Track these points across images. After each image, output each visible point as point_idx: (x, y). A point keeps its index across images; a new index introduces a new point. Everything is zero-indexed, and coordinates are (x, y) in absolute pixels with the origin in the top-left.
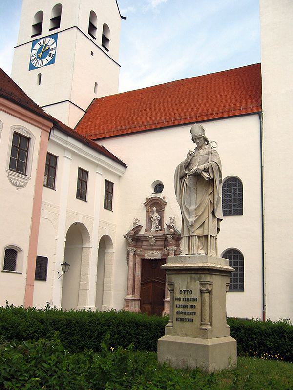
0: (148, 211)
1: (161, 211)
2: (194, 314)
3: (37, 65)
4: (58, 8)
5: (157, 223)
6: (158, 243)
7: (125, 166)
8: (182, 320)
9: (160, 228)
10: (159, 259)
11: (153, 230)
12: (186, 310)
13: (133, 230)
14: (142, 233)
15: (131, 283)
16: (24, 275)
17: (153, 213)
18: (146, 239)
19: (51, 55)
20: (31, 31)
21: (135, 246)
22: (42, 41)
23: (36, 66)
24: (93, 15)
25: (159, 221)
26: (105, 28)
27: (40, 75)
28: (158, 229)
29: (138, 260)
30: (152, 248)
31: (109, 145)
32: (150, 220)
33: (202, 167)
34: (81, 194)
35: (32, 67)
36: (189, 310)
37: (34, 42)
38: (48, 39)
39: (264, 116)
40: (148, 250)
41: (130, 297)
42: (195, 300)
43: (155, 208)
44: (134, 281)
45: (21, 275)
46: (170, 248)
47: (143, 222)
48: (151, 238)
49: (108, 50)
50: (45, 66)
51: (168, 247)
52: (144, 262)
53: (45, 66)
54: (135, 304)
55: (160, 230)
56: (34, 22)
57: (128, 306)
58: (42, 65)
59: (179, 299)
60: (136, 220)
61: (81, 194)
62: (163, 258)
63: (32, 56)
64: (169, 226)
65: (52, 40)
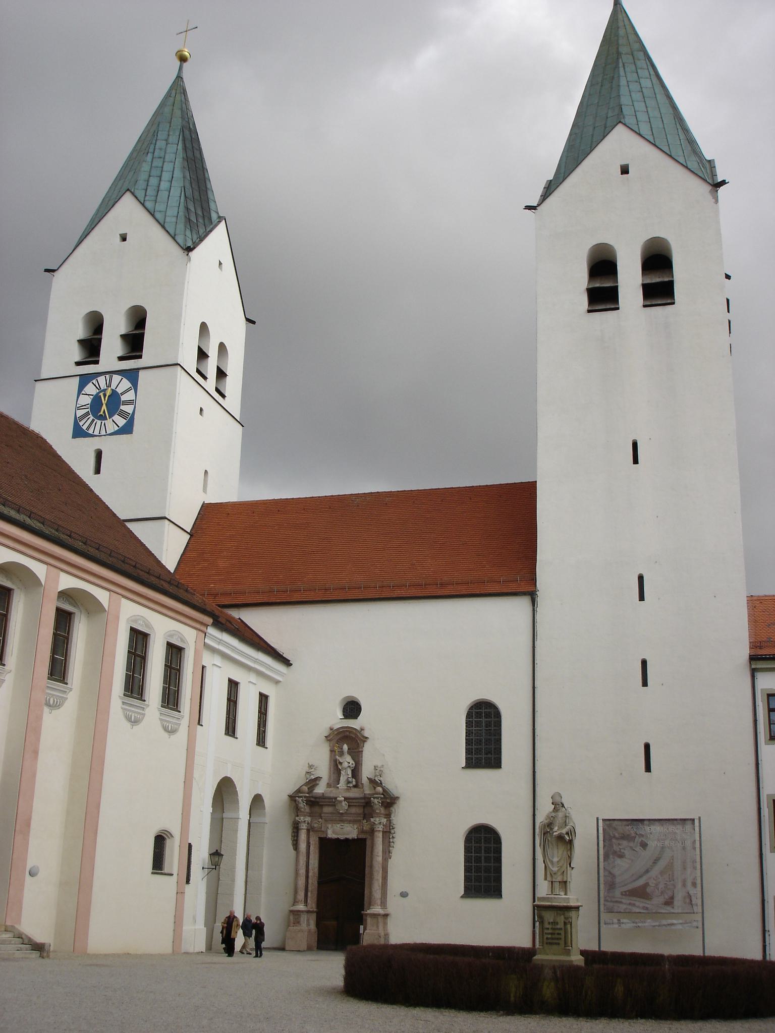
0: (332, 751)
2: (561, 939)
3: (88, 428)
4: (138, 318)
5: (349, 772)
6: (353, 810)
7: (287, 663)
8: (551, 944)
9: (354, 783)
10: (353, 840)
11: (342, 784)
12: (554, 936)
13: (306, 784)
14: (320, 789)
15: (302, 882)
17: (342, 754)
18: (332, 802)
19: (123, 414)
20: (77, 354)
21: (311, 815)
22: (102, 380)
23: (91, 431)
24: (204, 327)
25: (352, 770)
26: (222, 347)
27: (99, 455)
28: (351, 785)
29: (314, 841)
30: (341, 818)
31: (256, 619)
32: (336, 769)
33: (564, 831)
34: (231, 729)
35: (79, 432)
36: (556, 936)
37: (85, 380)
38: (116, 378)
39: (540, 600)
40: (333, 821)
41: (301, 907)
42: (561, 929)
43: (345, 747)
44: (307, 877)
45: (171, 877)
46: (376, 820)
47: (323, 770)
48: (341, 802)
49: (223, 396)
50: (110, 434)
51: (372, 820)
52: (326, 845)
53: (110, 434)
54: (308, 920)
55: (355, 786)
56: (81, 332)
57: (299, 922)
58: (103, 432)
59: (548, 929)
60: (311, 767)
61: (231, 729)
62: (360, 837)
64: (372, 781)
65: (126, 384)
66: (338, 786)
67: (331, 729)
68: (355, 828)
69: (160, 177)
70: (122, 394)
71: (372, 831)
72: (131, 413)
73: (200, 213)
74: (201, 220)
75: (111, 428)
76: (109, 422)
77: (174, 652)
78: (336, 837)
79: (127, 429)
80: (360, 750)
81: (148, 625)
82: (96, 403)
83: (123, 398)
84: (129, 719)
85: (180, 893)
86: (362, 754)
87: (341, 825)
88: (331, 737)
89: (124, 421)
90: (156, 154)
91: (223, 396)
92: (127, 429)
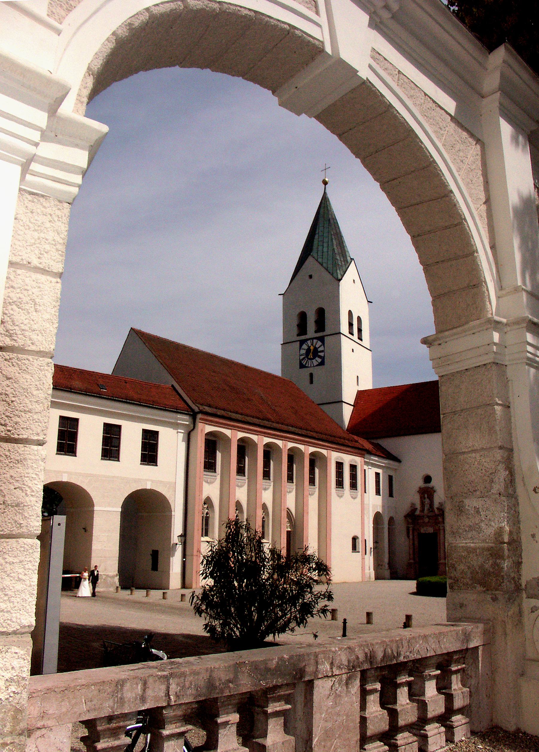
1: (431, 498)
4: (321, 312)
7: (399, 461)
11: (426, 511)
14: (418, 513)
16: (360, 553)
19: (320, 357)
22: (309, 342)
23: (307, 365)
26: (359, 319)
27: (311, 375)
29: (416, 534)
32: (423, 504)
34: (378, 492)
35: (302, 366)
37: (302, 342)
38: (315, 341)
41: (412, 561)
43: (426, 495)
47: (418, 506)
49: (361, 340)
63: (300, 355)
65: (319, 343)
67: (420, 488)
69: (323, 246)
70: (319, 347)
71: (439, 530)
72: (323, 356)
73: (342, 260)
74: (343, 263)
75: (315, 363)
76: (314, 361)
77: (353, 468)
79: (322, 363)
81: (342, 459)
82: (308, 350)
83: (319, 350)
84: (338, 496)
85: (363, 559)
89: (321, 360)
90: (320, 234)
91: (361, 340)
92: (322, 363)
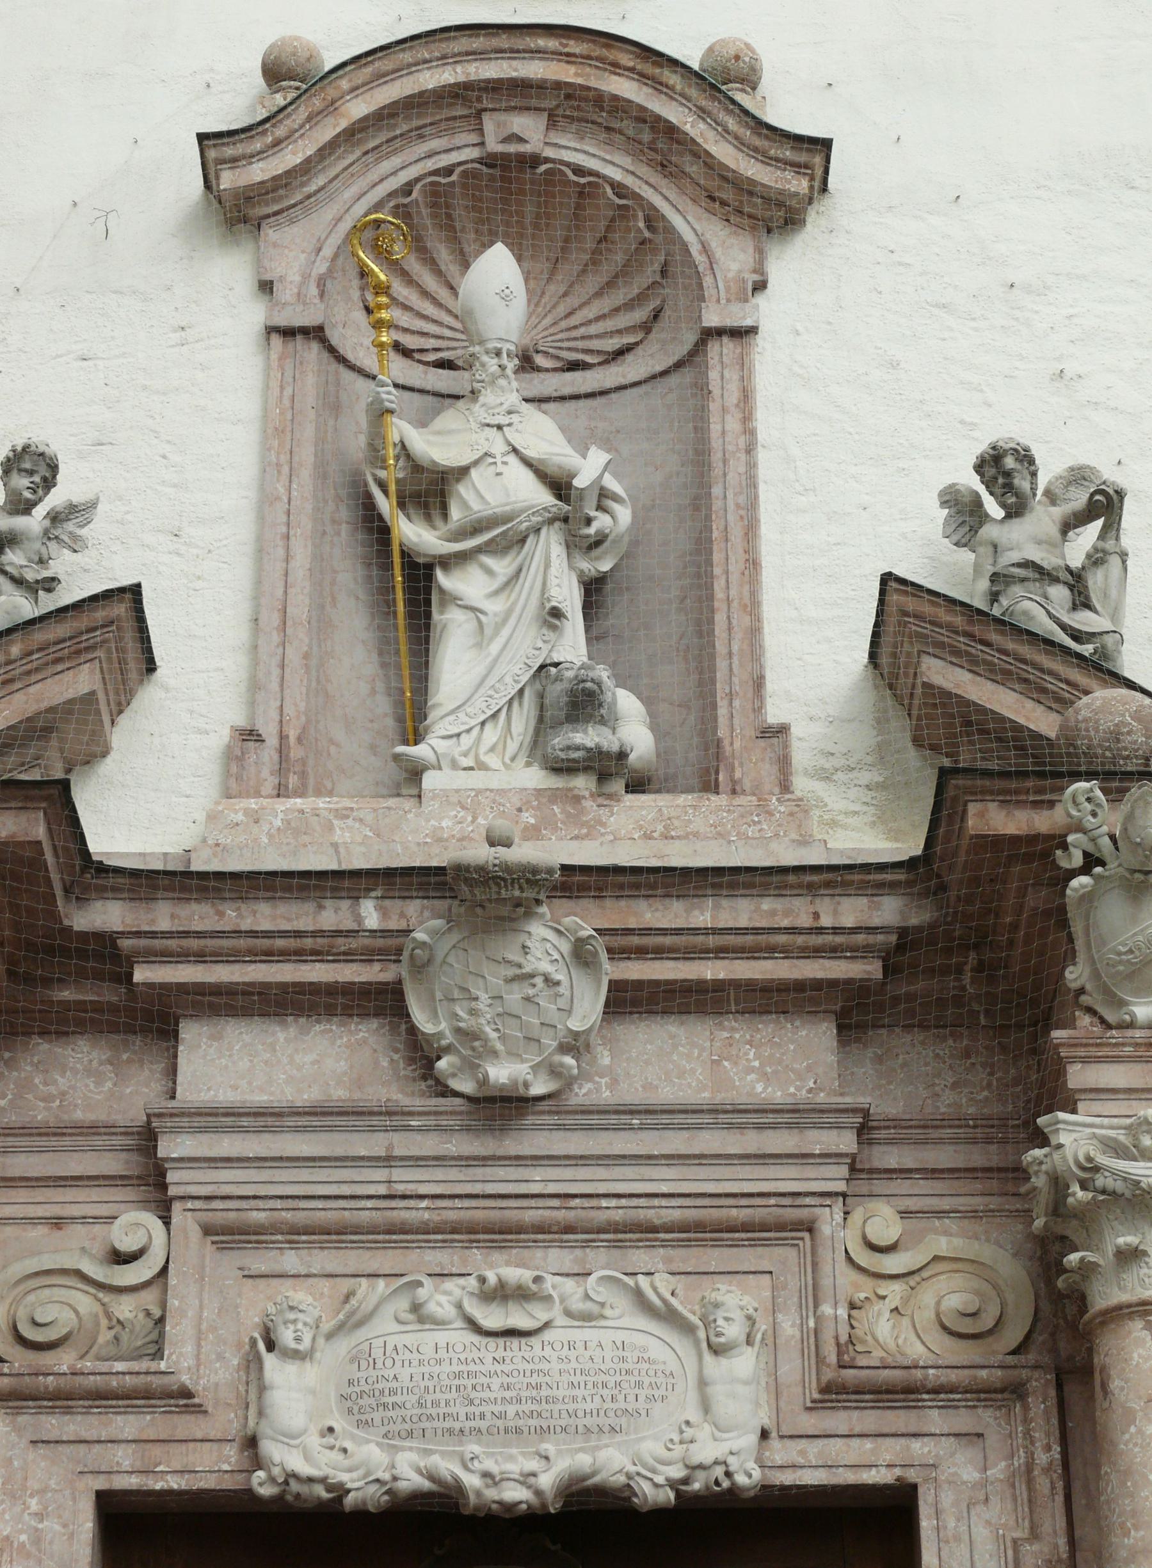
66: (420, 751)
68: (733, 1331)
78: (411, 1480)
80: (712, 318)
86: (744, 366)
87: (501, 1294)
88: (291, 158)
